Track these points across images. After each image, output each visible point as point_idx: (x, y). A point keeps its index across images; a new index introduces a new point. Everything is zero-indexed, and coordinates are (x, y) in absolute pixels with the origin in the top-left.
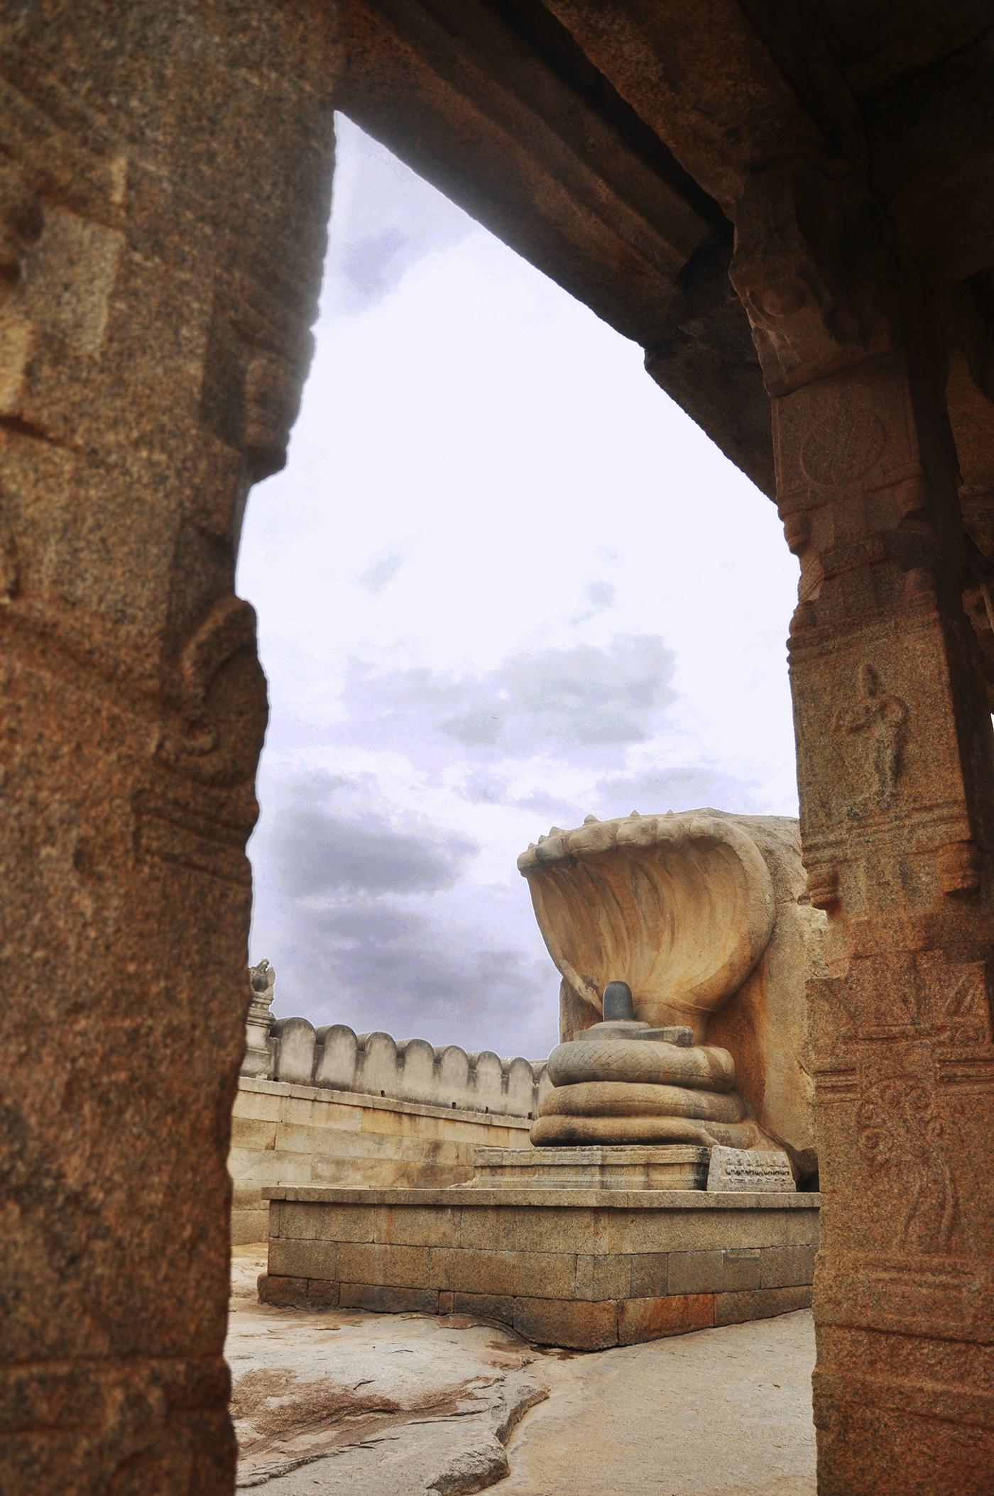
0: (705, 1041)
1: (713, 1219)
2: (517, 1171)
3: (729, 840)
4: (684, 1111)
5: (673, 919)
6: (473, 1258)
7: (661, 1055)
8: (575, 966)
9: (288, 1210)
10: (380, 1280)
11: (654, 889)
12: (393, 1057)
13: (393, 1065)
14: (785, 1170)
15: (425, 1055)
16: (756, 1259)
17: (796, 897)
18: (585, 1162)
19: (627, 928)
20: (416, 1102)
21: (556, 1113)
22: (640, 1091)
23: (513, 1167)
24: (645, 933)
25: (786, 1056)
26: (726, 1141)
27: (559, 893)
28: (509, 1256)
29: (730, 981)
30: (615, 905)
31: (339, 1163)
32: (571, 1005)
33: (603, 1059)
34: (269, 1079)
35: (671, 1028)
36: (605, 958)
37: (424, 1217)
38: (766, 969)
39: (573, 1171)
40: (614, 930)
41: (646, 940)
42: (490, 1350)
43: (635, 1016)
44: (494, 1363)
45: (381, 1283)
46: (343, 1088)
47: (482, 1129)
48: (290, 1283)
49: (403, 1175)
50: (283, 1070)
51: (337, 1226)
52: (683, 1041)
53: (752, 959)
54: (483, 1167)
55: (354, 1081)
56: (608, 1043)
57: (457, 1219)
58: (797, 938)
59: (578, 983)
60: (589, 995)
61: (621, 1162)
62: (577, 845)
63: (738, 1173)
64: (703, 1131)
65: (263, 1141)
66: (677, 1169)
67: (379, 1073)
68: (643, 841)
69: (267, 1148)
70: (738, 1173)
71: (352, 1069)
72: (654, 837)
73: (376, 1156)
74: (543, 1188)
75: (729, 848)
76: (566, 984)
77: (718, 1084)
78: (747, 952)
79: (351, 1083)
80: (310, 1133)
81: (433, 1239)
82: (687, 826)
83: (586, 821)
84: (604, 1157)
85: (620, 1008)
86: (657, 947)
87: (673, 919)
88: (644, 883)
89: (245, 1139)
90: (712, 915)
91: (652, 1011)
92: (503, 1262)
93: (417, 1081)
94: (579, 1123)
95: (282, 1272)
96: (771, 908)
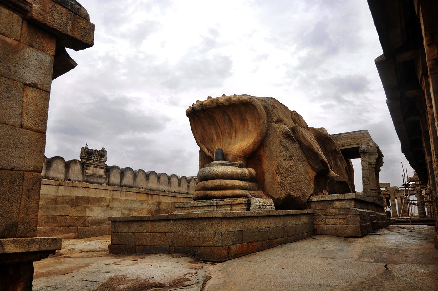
0: (246, 167)
1: (255, 219)
2: (189, 208)
3: (254, 103)
4: (242, 187)
5: (236, 129)
6: (180, 235)
7: (234, 171)
8: (204, 145)
9: (117, 224)
10: (149, 244)
11: (230, 119)
12: (145, 177)
13: (145, 179)
14: (272, 204)
15: (155, 176)
16: (267, 231)
17: (274, 121)
18: (211, 204)
19: (221, 132)
20: (153, 190)
21: (201, 190)
22: (228, 182)
23: (188, 207)
24: (227, 134)
25: (272, 170)
26: (254, 196)
27: (199, 122)
28: (192, 234)
29: (254, 147)
30: (217, 125)
31: (130, 210)
32: (203, 157)
33: (216, 172)
34: (106, 185)
35: (237, 162)
36: (214, 142)
37: (163, 223)
38: (265, 144)
39: (207, 207)
40: (217, 133)
41: (227, 135)
42: (189, 263)
43: (224, 159)
44: (192, 268)
45: (150, 245)
46: (130, 187)
47: (173, 198)
48: (119, 246)
49: (150, 213)
50: (111, 182)
51: (134, 228)
52: (240, 166)
53: (261, 140)
54: (178, 208)
55: (133, 184)
56: (217, 168)
57: (174, 224)
58: (275, 134)
59: (205, 150)
60: (209, 154)
61: (223, 204)
62: (206, 105)
63: (259, 206)
64: (248, 193)
65: (105, 204)
66: (240, 205)
67: (141, 182)
68: (227, 104)
69: (107, 206)
70: (259, 206)
71: (132, 181)
72: (230, 102)
73: (141, 207)
74: (199, 212)
75: (254, 106)
76: (201, 151)
77: (250, 179)
78: (260, 138)
79: (132, 185)
80: (120, 201)
81: (167, 230)
82: (240, 99)
83: (208, 98)
84: (217, 203)
85: (220, 157)
86: (231, 138)
87: (236, 129)
88: (227, 118)
89: (100, 204)
90: (248, 127)
91: (230, 158)
92: (190, 236)
93: (153, 184)
94: (209, 192)
95: (116, 243)
96: (267, 125)
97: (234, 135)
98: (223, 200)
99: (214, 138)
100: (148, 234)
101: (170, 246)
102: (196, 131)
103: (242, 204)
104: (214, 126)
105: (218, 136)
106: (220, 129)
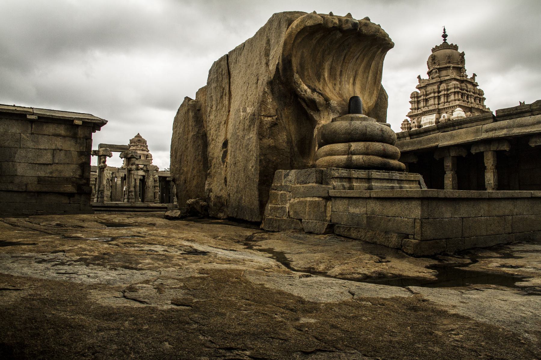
2: (359, 180)
19: (341, 71)
23: (357, 178)
37: (503, 204)
54: (337, 178)
81: (507, 212)
90: (367, 78)
97: (351, 81)
98: (402, 174)
99: (324, 75)
100: (483, 218)
101: (509, 233)
102: (296, 52)
103: (416, 181)
104: (333, 57)
105: (330, 74)
106: (342, 66)
